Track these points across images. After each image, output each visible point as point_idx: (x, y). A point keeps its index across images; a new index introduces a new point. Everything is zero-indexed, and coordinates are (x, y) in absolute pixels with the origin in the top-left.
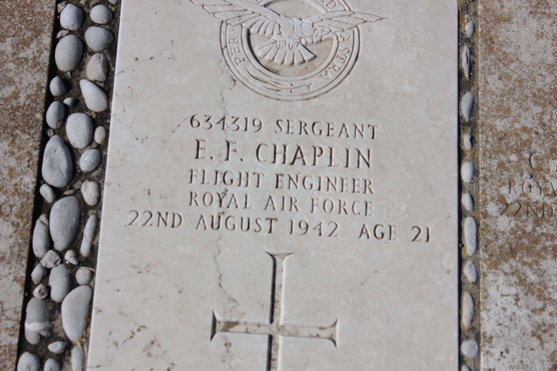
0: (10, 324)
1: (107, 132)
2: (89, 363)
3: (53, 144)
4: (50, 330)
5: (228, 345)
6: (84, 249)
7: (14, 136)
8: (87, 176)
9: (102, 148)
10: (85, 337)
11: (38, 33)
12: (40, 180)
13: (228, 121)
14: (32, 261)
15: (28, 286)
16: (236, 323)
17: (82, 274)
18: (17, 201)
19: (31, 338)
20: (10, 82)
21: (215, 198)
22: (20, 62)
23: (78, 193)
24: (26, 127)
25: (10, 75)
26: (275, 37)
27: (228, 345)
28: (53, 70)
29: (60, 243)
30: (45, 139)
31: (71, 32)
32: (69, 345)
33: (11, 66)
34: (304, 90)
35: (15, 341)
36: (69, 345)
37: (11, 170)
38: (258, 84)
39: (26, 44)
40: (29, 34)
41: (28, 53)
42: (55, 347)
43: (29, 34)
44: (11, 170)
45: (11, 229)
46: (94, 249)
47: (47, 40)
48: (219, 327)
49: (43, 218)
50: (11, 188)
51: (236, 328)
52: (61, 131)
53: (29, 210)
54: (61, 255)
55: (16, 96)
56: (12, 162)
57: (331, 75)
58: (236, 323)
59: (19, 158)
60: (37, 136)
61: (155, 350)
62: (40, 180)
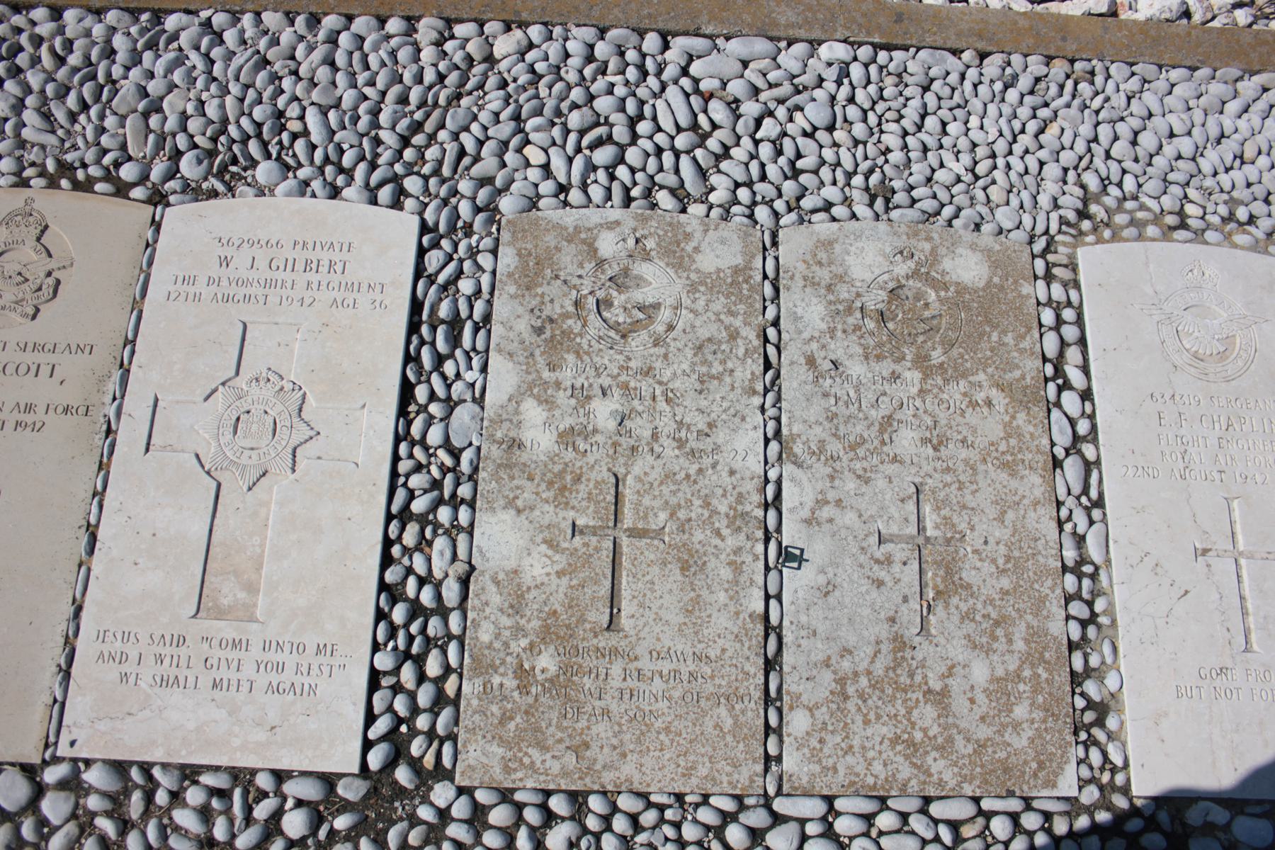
0: (1054, 552)
1: (1093, 405)
2: (1115, 581)
3: (1055, 414)
4: (1080, 555)
5: (1209, 566)
6: (1094, 494)
7: (1029, 409)
8: (1084, 439)
9: (1092, 417)
10: (1108, 561)
11: (1029, 329)
12: (1053, 444)
13: (1177, 398)
14: (1059, 504)
15: (1060, 524)
16: (1210, 550)
17: (1096, 514)
18: (1040, 458)
19: (1070, 563)
20: (1018, 367)
21: (1180, 456)
22: (1022, 351)
23: (1079, 452)
24: (1036, 402)
25: (1016, 361)
26: (1196, 334)
27: (1209, 566)
28: (1045, 359)
29: (1076, 489)
30: (1049, 411)
31: (1050, 329)
32: (1097, 568)
33: (1015, 354)
34: (1224, 374)
35: (1059, 564)
36: (1097, 568)
37: (1032, 434)
38: (1193, 370)
39: (1023, 337)
40: (1023, 330)
41: (1025, 344)
42: (1088, 569)
43: (1023, 330)
44: (1032, 434)
45: (1040, 480)
46: (1101, 495)
47: (1037, 335)
48: (1199, 552)
49: (1058, 471)
50: (1034, 449)
51: (1210, 553)
52: (1058, 404)
53: (1050, 465)
54: (1078, 498)
55: (1023, 377)
56: (1031, 429)
57: (1240, 363)
58: (1210, 550)
59: (1035, 425)
60: (1045, 408)
61: (1159, 570)
62: (1053, 444)
